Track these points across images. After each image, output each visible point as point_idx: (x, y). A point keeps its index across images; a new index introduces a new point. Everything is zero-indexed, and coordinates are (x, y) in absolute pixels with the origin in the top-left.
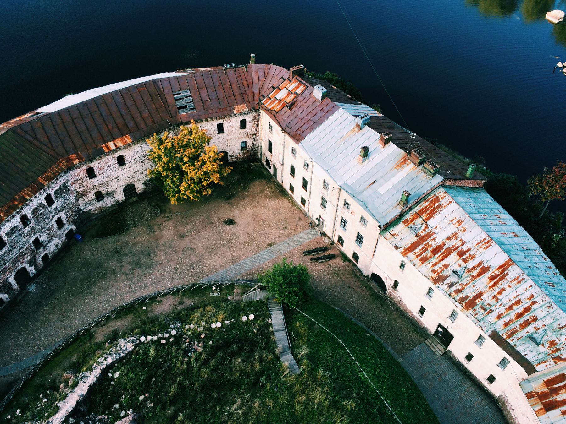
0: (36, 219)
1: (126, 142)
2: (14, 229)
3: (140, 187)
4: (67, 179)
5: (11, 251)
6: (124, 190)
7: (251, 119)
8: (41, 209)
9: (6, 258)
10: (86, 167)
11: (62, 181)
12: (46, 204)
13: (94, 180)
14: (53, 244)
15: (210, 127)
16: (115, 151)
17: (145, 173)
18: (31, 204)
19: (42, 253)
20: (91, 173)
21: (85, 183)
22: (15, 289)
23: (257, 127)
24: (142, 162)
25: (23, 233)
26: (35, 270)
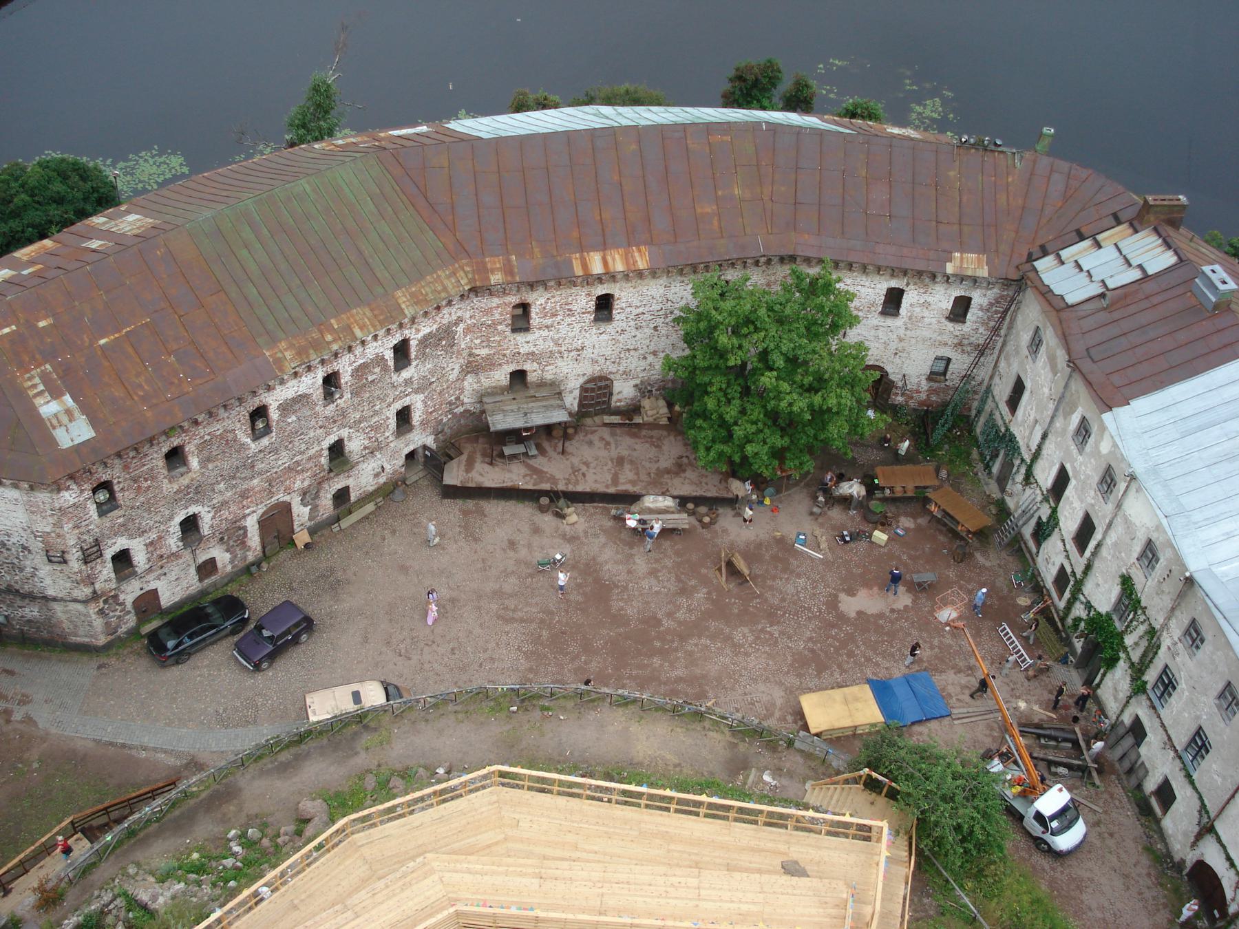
0: (355, 394)
1: (635, 262)
2: (302, 399)
3: (624, 391)
4: (459, 313)
6: (583, 389)
7: (985, 302)
8: (377, 370)
9: (259, 466)
10: (514, 299)
11: (447, 316)
12: (391, 363)
13: (521, 338)
14: (370, 467)
15: (866, 291)
16: (600, 279)
17: (650, 358)
18: (358, 350)
19: (338, 484)
20: (521, 318)
21: (497, 338)
22: (249, 549)
23: (995, 331)
24: (655, 328)
25: (316, 415)
26: (309, 519)
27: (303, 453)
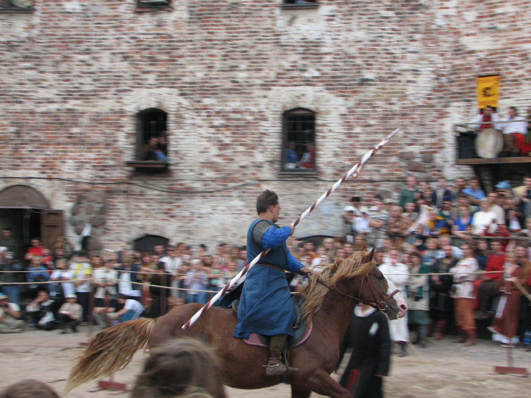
5: (34, 59)
27: (84, 97)
